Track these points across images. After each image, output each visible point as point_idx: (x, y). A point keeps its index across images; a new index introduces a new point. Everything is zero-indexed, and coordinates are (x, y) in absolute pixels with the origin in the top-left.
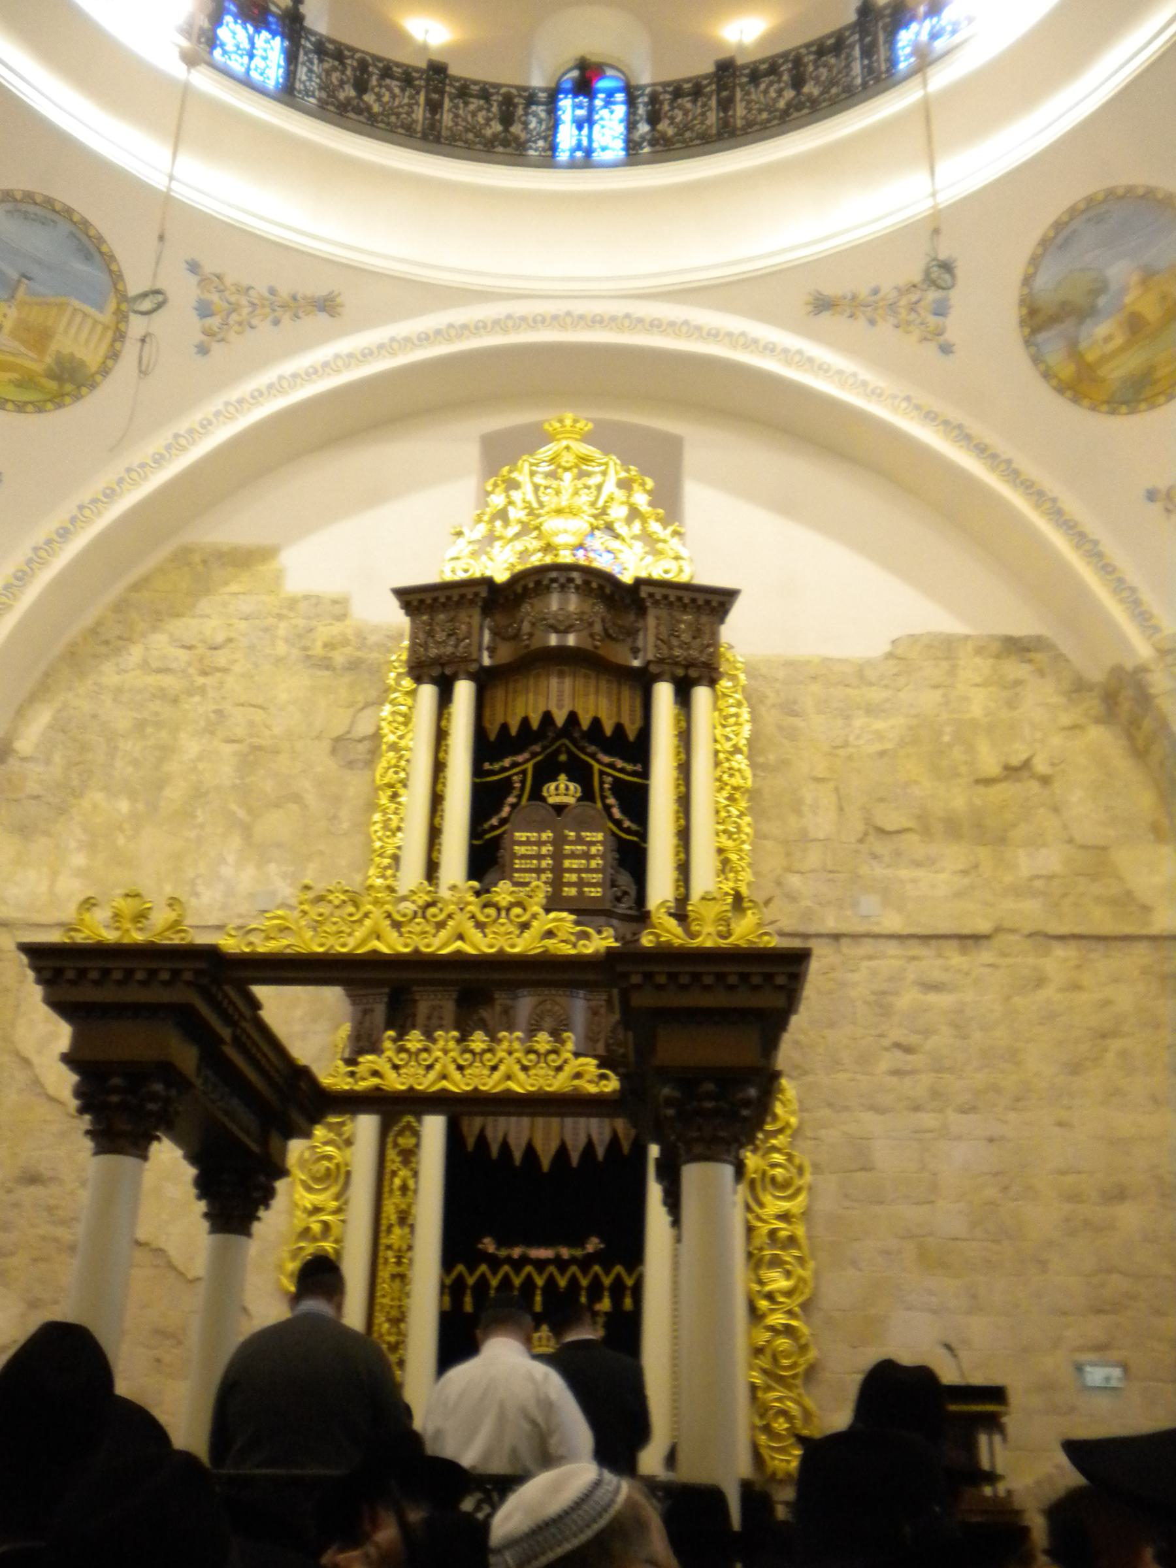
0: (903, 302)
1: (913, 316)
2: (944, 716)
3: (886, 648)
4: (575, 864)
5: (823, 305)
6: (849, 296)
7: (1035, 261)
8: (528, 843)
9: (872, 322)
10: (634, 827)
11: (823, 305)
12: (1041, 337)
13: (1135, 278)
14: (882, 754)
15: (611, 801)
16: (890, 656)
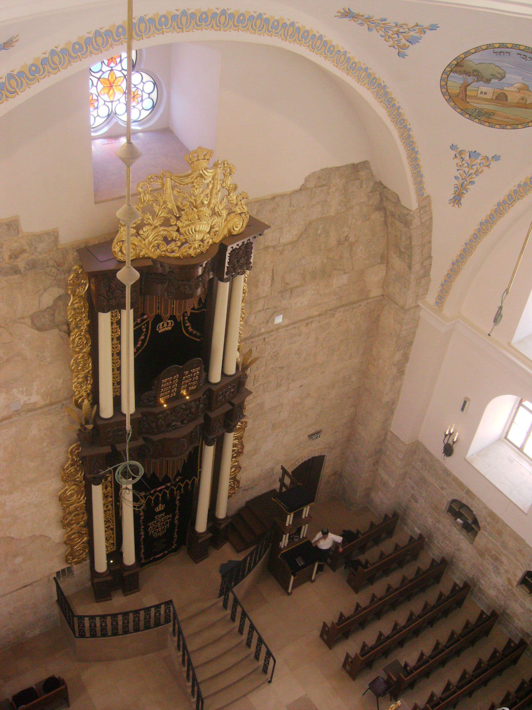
0: (396, 29)
1: (396, 36)
2: (320, 217)
3: (302, 182)
4: (187, 381)
5: (348, 14)
6: (366, 16)
7: (477, 50)
8: (168, 381)
9: (369, 29)
10: (198, 334)
11: (348, 14)
12: (452, 74)
13: (518, 85)
14: (293, 244)
15: (188, 324)
16: (303, 189)
